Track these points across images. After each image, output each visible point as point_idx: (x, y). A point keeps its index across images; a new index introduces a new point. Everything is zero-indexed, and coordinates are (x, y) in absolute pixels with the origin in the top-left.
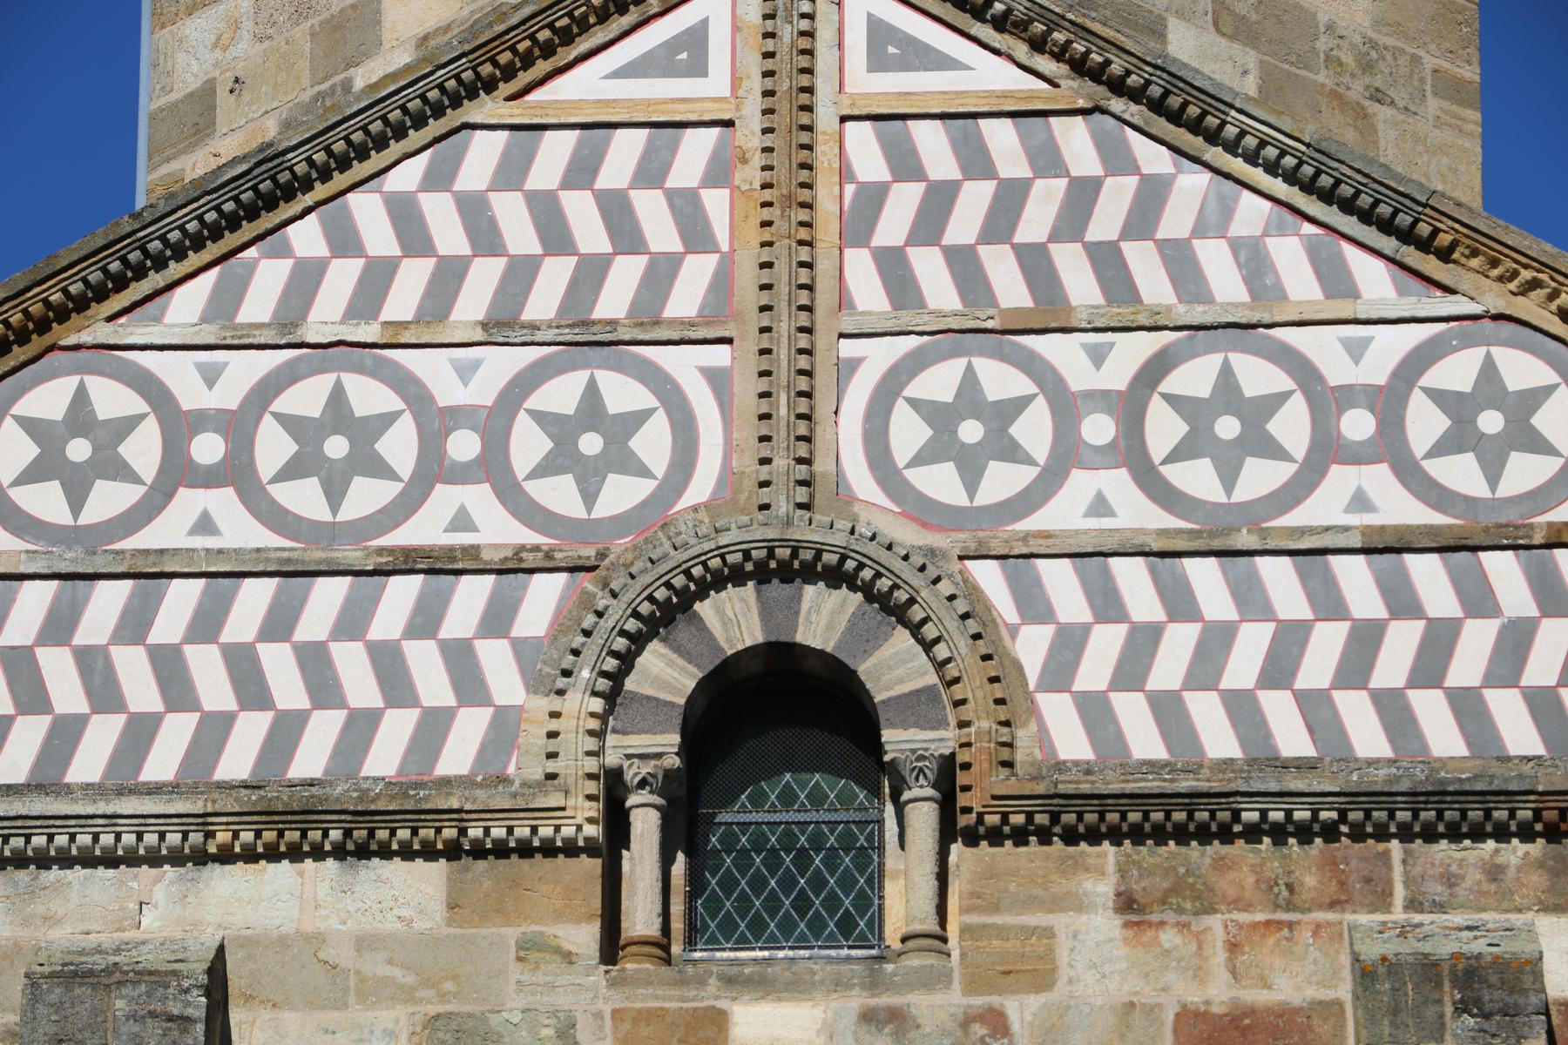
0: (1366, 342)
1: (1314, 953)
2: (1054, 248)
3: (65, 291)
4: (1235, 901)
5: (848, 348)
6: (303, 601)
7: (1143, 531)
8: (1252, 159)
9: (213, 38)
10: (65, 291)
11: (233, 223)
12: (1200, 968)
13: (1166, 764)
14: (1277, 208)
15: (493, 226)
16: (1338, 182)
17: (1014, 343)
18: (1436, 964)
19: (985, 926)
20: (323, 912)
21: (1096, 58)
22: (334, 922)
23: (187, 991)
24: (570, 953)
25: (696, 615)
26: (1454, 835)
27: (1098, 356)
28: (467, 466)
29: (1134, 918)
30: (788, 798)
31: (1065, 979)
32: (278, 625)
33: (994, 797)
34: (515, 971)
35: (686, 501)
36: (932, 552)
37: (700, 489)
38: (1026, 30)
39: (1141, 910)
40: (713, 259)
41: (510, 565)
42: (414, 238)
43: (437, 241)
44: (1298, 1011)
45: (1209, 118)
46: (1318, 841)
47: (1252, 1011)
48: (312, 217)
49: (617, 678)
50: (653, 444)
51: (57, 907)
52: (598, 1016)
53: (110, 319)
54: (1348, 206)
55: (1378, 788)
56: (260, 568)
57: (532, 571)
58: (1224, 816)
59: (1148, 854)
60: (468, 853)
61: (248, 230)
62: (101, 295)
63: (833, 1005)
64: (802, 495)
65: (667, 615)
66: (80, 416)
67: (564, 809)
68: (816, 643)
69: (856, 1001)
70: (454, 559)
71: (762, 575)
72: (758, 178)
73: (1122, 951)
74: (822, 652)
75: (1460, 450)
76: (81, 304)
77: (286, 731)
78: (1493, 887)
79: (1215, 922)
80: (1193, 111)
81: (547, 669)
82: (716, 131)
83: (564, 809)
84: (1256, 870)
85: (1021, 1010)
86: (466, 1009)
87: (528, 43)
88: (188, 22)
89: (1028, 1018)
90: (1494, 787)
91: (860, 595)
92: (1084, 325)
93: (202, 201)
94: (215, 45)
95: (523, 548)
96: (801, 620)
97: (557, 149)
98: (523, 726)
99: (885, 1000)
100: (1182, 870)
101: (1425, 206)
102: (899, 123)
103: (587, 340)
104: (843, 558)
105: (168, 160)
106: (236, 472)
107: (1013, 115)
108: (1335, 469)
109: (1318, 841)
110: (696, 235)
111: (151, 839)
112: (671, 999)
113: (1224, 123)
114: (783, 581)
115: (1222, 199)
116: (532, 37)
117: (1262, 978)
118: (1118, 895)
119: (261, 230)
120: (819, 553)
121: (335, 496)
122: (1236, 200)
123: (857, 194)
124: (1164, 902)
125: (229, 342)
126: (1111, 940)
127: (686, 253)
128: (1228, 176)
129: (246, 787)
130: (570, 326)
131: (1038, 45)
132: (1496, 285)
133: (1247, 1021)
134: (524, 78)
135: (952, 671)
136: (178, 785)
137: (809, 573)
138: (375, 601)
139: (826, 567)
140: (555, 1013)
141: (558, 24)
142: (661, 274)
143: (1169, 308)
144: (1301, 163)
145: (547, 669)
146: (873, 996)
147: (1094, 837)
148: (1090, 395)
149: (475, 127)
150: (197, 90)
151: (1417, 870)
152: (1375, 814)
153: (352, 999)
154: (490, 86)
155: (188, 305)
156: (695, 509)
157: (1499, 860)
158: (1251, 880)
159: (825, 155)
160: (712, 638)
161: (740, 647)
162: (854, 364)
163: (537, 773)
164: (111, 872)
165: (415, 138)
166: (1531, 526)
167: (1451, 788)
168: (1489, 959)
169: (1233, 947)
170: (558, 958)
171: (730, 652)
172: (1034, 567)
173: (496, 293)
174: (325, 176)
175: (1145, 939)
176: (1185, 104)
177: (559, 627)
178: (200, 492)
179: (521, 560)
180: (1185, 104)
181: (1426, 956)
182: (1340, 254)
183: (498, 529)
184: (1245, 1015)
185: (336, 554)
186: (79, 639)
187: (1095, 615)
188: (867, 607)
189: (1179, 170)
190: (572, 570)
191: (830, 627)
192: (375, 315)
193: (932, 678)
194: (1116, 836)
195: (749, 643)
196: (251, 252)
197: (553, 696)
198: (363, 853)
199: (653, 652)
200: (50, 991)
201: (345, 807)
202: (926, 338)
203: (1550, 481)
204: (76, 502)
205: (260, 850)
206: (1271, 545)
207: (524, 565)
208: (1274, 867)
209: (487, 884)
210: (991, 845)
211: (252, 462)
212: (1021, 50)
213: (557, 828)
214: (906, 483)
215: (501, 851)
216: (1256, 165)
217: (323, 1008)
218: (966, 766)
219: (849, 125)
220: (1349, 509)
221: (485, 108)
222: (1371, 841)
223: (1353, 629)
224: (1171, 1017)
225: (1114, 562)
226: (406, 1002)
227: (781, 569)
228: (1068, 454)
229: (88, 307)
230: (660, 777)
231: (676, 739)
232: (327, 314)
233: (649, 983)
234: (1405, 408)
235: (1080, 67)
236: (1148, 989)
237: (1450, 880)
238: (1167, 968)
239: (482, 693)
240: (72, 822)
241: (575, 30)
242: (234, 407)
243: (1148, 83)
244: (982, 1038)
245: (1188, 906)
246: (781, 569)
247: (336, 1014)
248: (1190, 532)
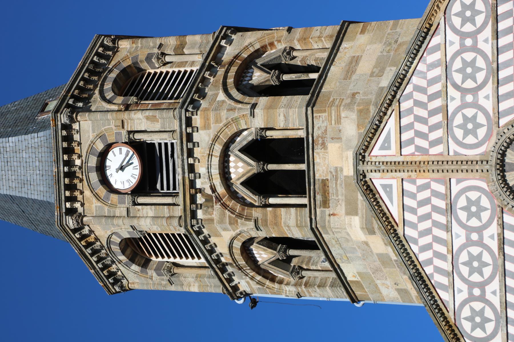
0: (450, 41)
2: (429, 109)
3: (442, 321)
5: (451, 153)
7: (493, 88)
8: (410, 67)
11: (426, 285)
16: (415, 49)
25: (513, 186)
27: (453, 99)
28: (479, 236)
36: (498, 134)
40: (432, 183)
43: (429, 242)
48: (424, 269)
50: (473, 195)
53: (448, 312)
54: (420, 47)
57: (503, 222)
61: (428, 282)
62: (443, 314)
64: (484, 163)
66: (470, 319)
70: (501, 239)
71: (503, 171)
72: (414, 173)
75: (474, 20)
76: (445, 318)
80: (399, 80)
82: (404, 182)
87: (386, 222)
95: (498, 224)
97: (408, 216)
102: (402, 143)
103: (450, 209)
104: (499, 153)
106: (482, 286)
110: (427, 186)
113: (402, 74)
115: (418, 74)
116: (385, 221)
120: (498, 159)
121: (487, 265)
122: (419, 70)
123: (417, 152)
128: (413, 72)
131: (385, 114)
134: (393, 223)
137: (503, 161)
142: (436, 194)
143: (442, 84)
148: (462, 100)
154: (395, 230)
155: (445, 296)
156: (488, 186)
159: (409, 159)
162: (455, 152)
165: (407, 246)
166: (492, 4)
174: (415, 266)
176: (398, 82)
180: (398, 82)
182: (430, 48)
183: (494, 229)
189: (412, 83)
190: (503, 213)
192: (445, 256)
206: (496, 60)
211: (480, 282)
212: (386, 117)
214: (482, 140)
219: (402, 154)
220: (488, 43)
221: (400, 232)
225: (499, 94)
228: (475, 105)
232: (446, 266)
235: (390, 105)
243: (393, 90)
248: (493, 77)
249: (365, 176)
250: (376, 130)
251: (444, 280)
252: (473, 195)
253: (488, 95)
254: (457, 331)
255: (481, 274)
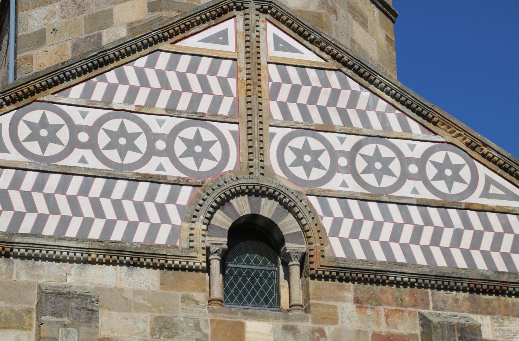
0: (414, 146)
1: (409, 320)
2: (328, 108)
3: (40, 84)
4: (387, 303)
5: (272, 130)
6: (114, 187)
7: (358, 193)
8: (382, 90)
9: (44, 16)
10: (40, 84)
11: (90, 70)
12: (378, 321)
13: (366, 261)
14: (389, 105)
15: (167, 80)
16: (407, 99)
17: (318, 134)
18: (453, 325)
19: (317, 304)
20: (123, 282)
21: (340, 55)
22: (126, 286)
23: (93, 302)
24: (197, 301)
25: (231, 203)
26: (445, 289)
27: (342, 141)
28: (162, 151)
29: (359, 305)
30: (248, 261)
31: (341, 321)
32: (106, 193)
33: (321, 266)
34: (181, 305)
35: (227, 169)
36: (298, 192)
37: (231, 166)
38: (319, 44)
39: (361, 303)
40: (232, 99)
41: (176, 183)
42: (144, 82)
43: (151, 83)
44: (406, 336)
45: (371, 76)
46: (409, 287)
47: (393, 335)
48: (113, 71)
49: (209, 219)
50: (216, 150)
51: (41, 273)
52: (206, 321)
53: (53, 94)
54: (408, 107)
55: (427, 273)
56: (101, 175)
57: (182, 185)
58: (384, 278)
59: (362, 286)
60: (166, 268)
61: (94, 73)
62: (50, 86)
63: (275, 324)
65: (223, 203)
66: (43, 122)
67: (196, 257)
68: (266, 215)
69: (281, 323)
70: (159, 179)
71: (250, 194)
73: (356, 315)
74: (267, 218)
75: (441, 179)
76: (44, 88)
77: (110, 226)
78: (456, 305)
79: (381, 308)
80: (367, 74)
81: (188, 215)
82: (231, 61)
83: (196, 257)
84: (392, 294)
85: (329, 329)
86: (167, 315)
87: (178, 28)
88: (34, 10)
89: (331, 332)
90: (458, 276)
91: (278, 202)
92: (338, 131)
93: (82, 62)
94: (45, 18)
95: (180, 178)
96: (261, 208)
97: (185, 61)
98: (182, 231)
99: (289, 323)
100: (372, 292)
101: (431, 109)
102: (283, 66)
103: (196, 118)
104: (275, 191)
105: (26, 51)
106: (92, 145)
107: (316, 68)
108: (408, 181)
109: (409, 287)
110: (227, 92)
111: (71, 254)
112: (228, 318)
113: (375, 78)
114: (256, 196)
115: (374, 100)
116: (179, 26)
117: (395, 326)
118: (355, 298)
119: (98, 73)
120: (268, 189)
121: (122, 156)
122: (378, 101)
123: (272, 85)
124: (367, 301)
125: (89, 105)
126: (353, 311)
127: (224, 96)
128: (375, 94)
129: (98, 241)
130: (191, 113)
131: (322, 49)
132: (449, 134)
133: (392, 338)
134: (175, 38)
135: (307, 227)
136: (77, 239)
137: (264, 195)
138: (135, 189)
139: (269, 193)
140: (193, 319)
141: (187, 24)
142: (217, 102)
143: (361, 129)
144: (397, 93)
145: (188, 215)
146: (286, 322)
147: (347, 280)
148: (340, 151)
149: (161, 51)
150: (38, 31)
151: (436, 298)
152: (426, 281)
153: (132, 310)
154: (166, 39)
155: (76, 92)
156: (230, 172)
157: (457, 297)
158: (391, 297)
160: (235, 211)
161: (244, 214)
162: (273, 135)
163: (186, 245)
164: (57, 264)
165: (144, 52)
166: (461, 203)
167: (446, 275)
168: (467, 325)
169: (387, 316)
170: (194, 302)
171: (241, 216)
172: (327, 200)
173: (169, 101)
174: (117, 59)
175: (362, 312)
176: (365, 72)
177: (191, 202)
178: (81, 150)
179: (179, 181)
180: (365, 72)
181: (450, 323)
182: (406, 119)
183: (171, 171)
184: (391, 336)
185: (125, 174)
186: (45, 191)
187: (344, 215)
188: (280, 206)
189: (362, 90)
190: (194, 186)
191: (270, 211)
192: (133, 103)
193: (299, 229)
194: (353, 281)
195: (246, 213)
196: (95, 79)
197: (190, 223)
198: (135, 265)
199: (219, 213)
200: (51, 298)
201: (131, 250)
202: (294, 129)
203: (465, 191)
204: (43, 148)
205: (111, 261)
206: (392, 201)
207: (180, 183)
208: (397, 294)
209: (172, 278)
210: (318, 280)
211: (97, 143)
212: (318, 50)
213: (194, 263)
214: (290, 171)
215: (176, 268)
216: (383, 91)
217: (124, 311)
218: (311, 256)
219: (269, 65)
220: (412, 193)
221: (164, 45)
222: (423, 289)
223: (414, 227)
224: (371, 335)
225: (349, 200)
226: (149, 312)
227: (256, 192)
228: (334, 169)
229: (46, 90)
230: (221, 251)
231: (226, 240)
233: (221, 312)
234: (425, 166)
235: (334, 57)
236: (364, 326)
237: (445, 302)
238: (369, 321)
239: (164, 219)
240: (48, 247)
241: (191, 26)
242: (91, 125)
243: (354, 64)
244: (318, 337)
245: (374, 303)
246: (256, 192)
247: (128, 313)
248: (370, 194)
249: (239, 9)
250: (301, 34)
251: (98, 95)
252: (216, 150)
253: (347, 187)
254: (25, 101)
255: (109, 147)
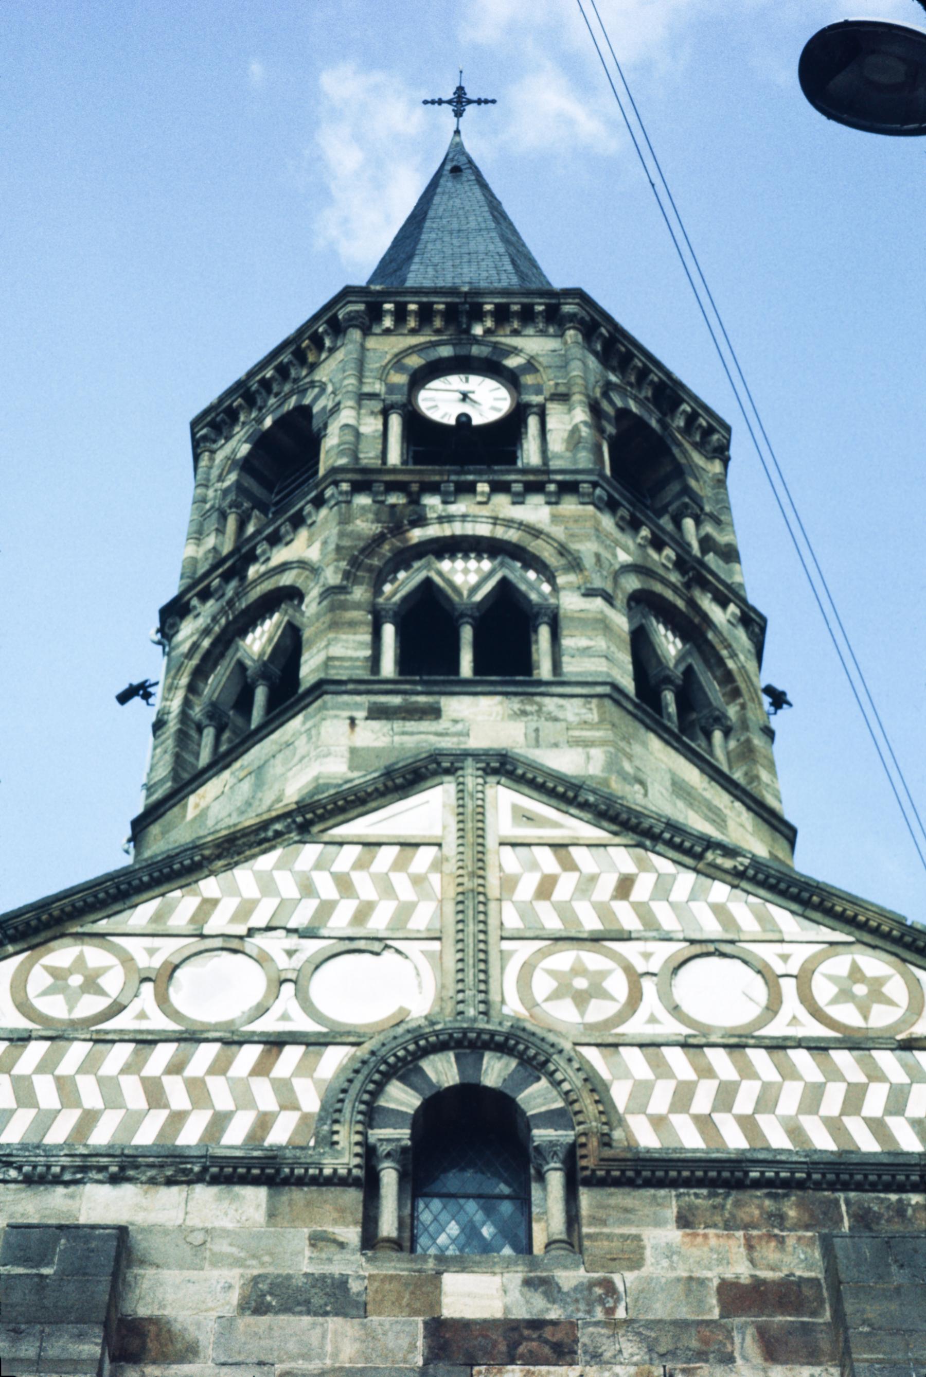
5: (506, 945)
29: (688, 1231)
64: (482, 1007)
159: (490, 859)
162: (511, 953)
218: (583, 1145)
231: (408, 1131)
232: (217, 923)
244: (600, 1296)
246: (469, 1044)
250: (562, 797)
251: (180, 919)
